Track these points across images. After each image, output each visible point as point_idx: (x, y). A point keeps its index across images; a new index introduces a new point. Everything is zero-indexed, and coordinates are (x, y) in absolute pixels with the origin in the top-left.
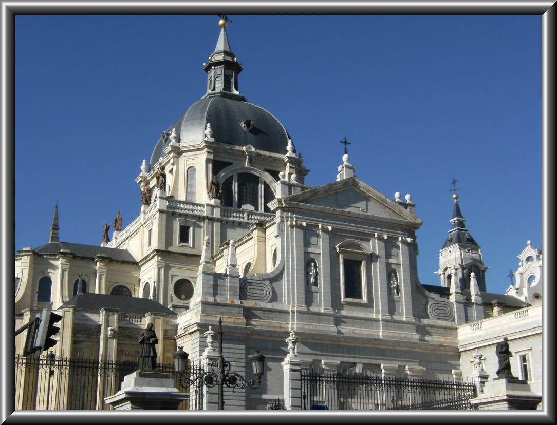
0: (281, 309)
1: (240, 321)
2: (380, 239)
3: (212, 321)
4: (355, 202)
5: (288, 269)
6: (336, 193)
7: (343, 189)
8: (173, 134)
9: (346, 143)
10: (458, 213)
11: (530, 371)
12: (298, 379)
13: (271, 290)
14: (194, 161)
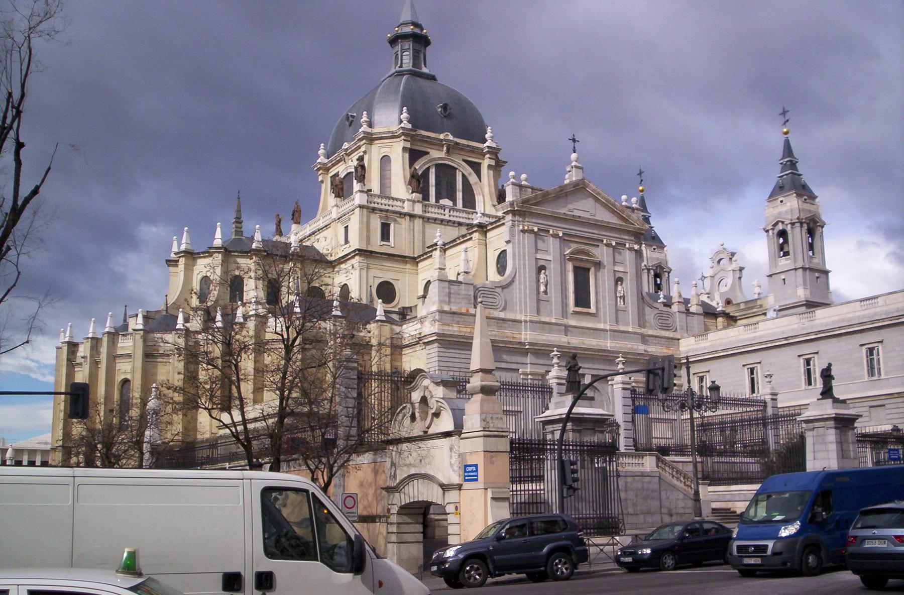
2: (608, 245)
8: (365, 118)
9: (574, 140)
11: (758, 383)
14: (388, 150)
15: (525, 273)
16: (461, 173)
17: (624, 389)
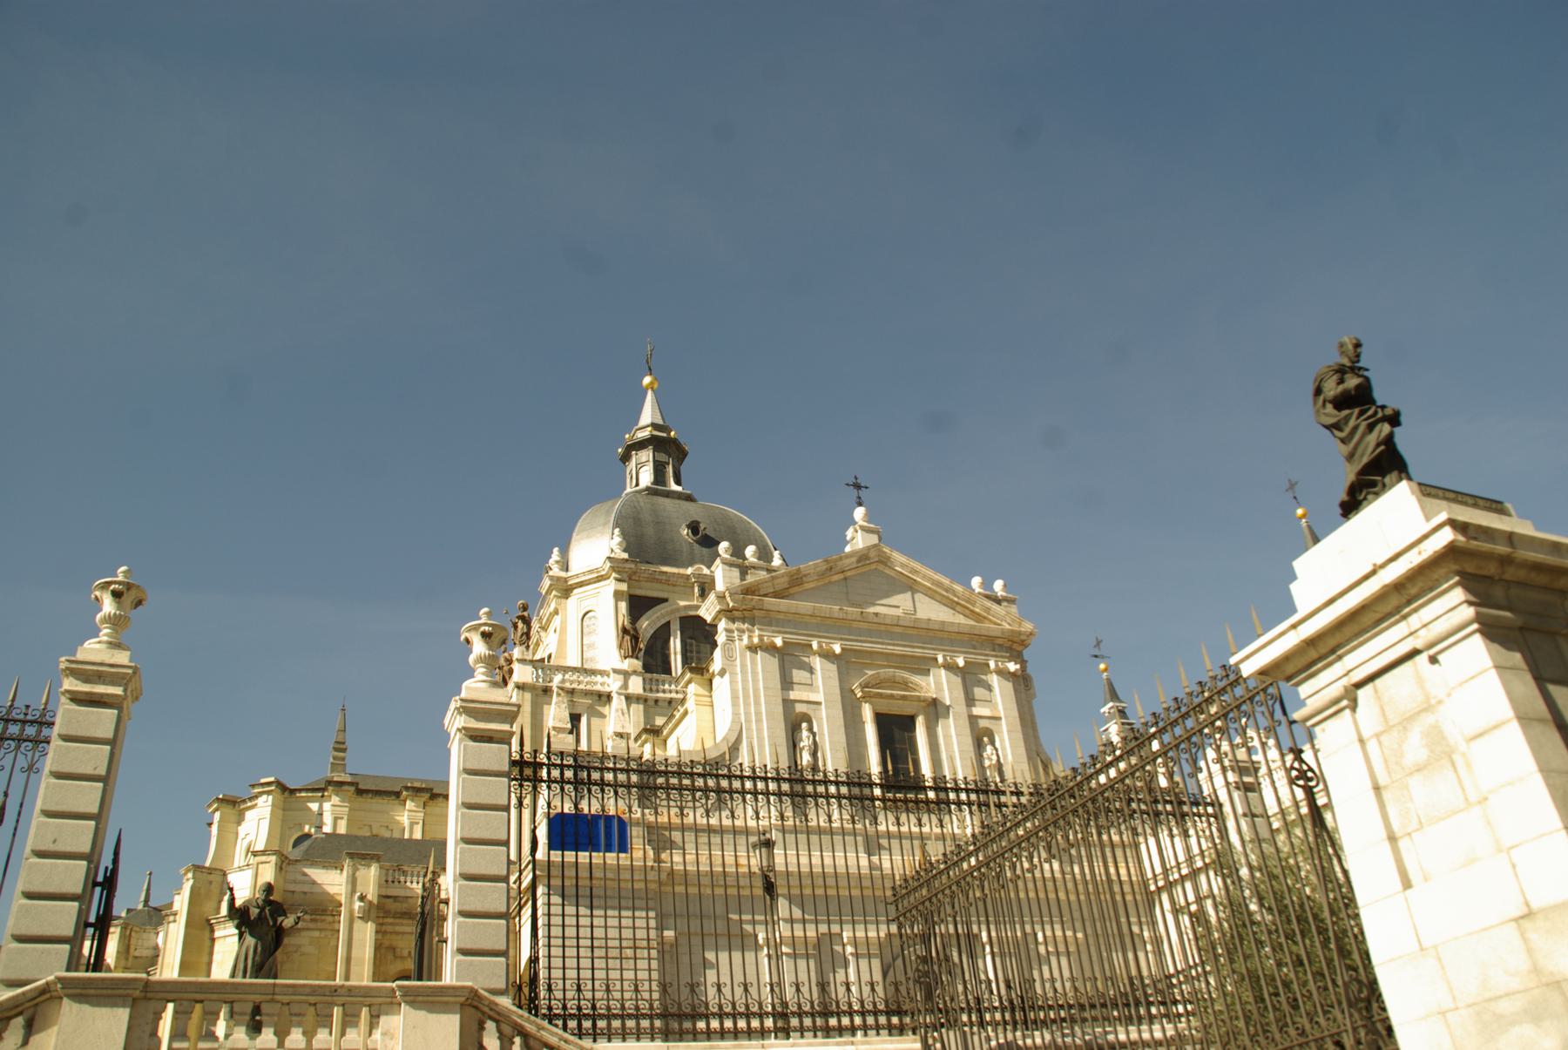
2: (950, 667)
4: (888, 596)
6: (845, 579)
9: (858, 486)
10: (1114, 696)
12: (495, 767)
15: (759, 730)
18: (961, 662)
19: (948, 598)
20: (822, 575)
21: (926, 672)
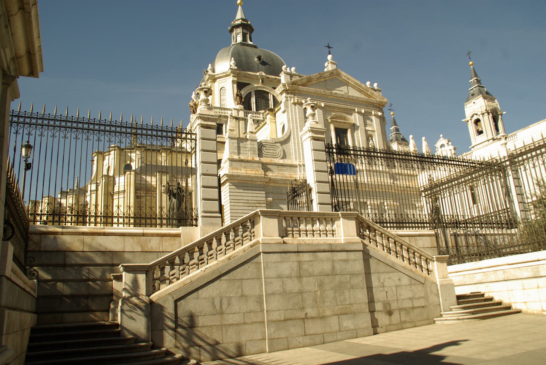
0: (291, 163)
1: (260, 173)
2: (359, 113)
3: (238, 173)
4: (339, 87)
5: (294, 134)
7: (330, 78)
9: (329, 47)
13: (282, 150)
16: (272, 95)
17: (315, 139)
18: (363, 111)
19: (359, 89)
20: (318, 79)
21: (351, 114)
